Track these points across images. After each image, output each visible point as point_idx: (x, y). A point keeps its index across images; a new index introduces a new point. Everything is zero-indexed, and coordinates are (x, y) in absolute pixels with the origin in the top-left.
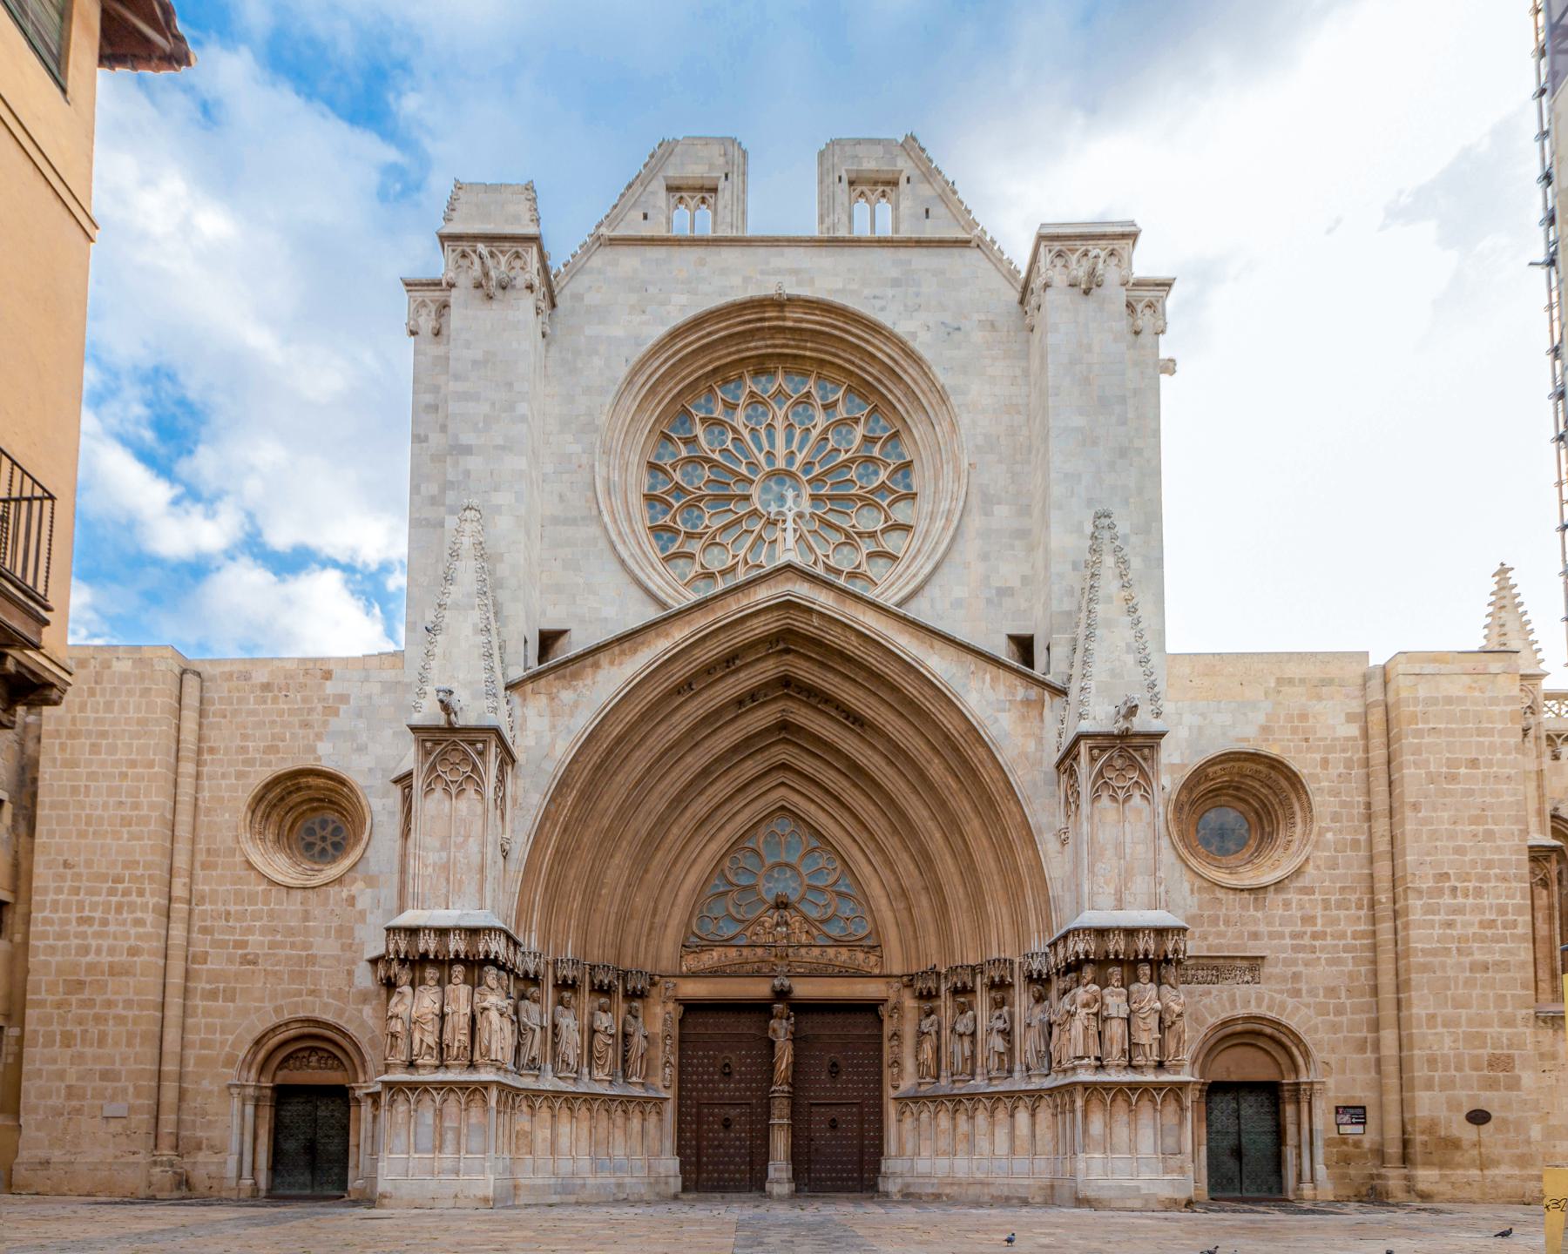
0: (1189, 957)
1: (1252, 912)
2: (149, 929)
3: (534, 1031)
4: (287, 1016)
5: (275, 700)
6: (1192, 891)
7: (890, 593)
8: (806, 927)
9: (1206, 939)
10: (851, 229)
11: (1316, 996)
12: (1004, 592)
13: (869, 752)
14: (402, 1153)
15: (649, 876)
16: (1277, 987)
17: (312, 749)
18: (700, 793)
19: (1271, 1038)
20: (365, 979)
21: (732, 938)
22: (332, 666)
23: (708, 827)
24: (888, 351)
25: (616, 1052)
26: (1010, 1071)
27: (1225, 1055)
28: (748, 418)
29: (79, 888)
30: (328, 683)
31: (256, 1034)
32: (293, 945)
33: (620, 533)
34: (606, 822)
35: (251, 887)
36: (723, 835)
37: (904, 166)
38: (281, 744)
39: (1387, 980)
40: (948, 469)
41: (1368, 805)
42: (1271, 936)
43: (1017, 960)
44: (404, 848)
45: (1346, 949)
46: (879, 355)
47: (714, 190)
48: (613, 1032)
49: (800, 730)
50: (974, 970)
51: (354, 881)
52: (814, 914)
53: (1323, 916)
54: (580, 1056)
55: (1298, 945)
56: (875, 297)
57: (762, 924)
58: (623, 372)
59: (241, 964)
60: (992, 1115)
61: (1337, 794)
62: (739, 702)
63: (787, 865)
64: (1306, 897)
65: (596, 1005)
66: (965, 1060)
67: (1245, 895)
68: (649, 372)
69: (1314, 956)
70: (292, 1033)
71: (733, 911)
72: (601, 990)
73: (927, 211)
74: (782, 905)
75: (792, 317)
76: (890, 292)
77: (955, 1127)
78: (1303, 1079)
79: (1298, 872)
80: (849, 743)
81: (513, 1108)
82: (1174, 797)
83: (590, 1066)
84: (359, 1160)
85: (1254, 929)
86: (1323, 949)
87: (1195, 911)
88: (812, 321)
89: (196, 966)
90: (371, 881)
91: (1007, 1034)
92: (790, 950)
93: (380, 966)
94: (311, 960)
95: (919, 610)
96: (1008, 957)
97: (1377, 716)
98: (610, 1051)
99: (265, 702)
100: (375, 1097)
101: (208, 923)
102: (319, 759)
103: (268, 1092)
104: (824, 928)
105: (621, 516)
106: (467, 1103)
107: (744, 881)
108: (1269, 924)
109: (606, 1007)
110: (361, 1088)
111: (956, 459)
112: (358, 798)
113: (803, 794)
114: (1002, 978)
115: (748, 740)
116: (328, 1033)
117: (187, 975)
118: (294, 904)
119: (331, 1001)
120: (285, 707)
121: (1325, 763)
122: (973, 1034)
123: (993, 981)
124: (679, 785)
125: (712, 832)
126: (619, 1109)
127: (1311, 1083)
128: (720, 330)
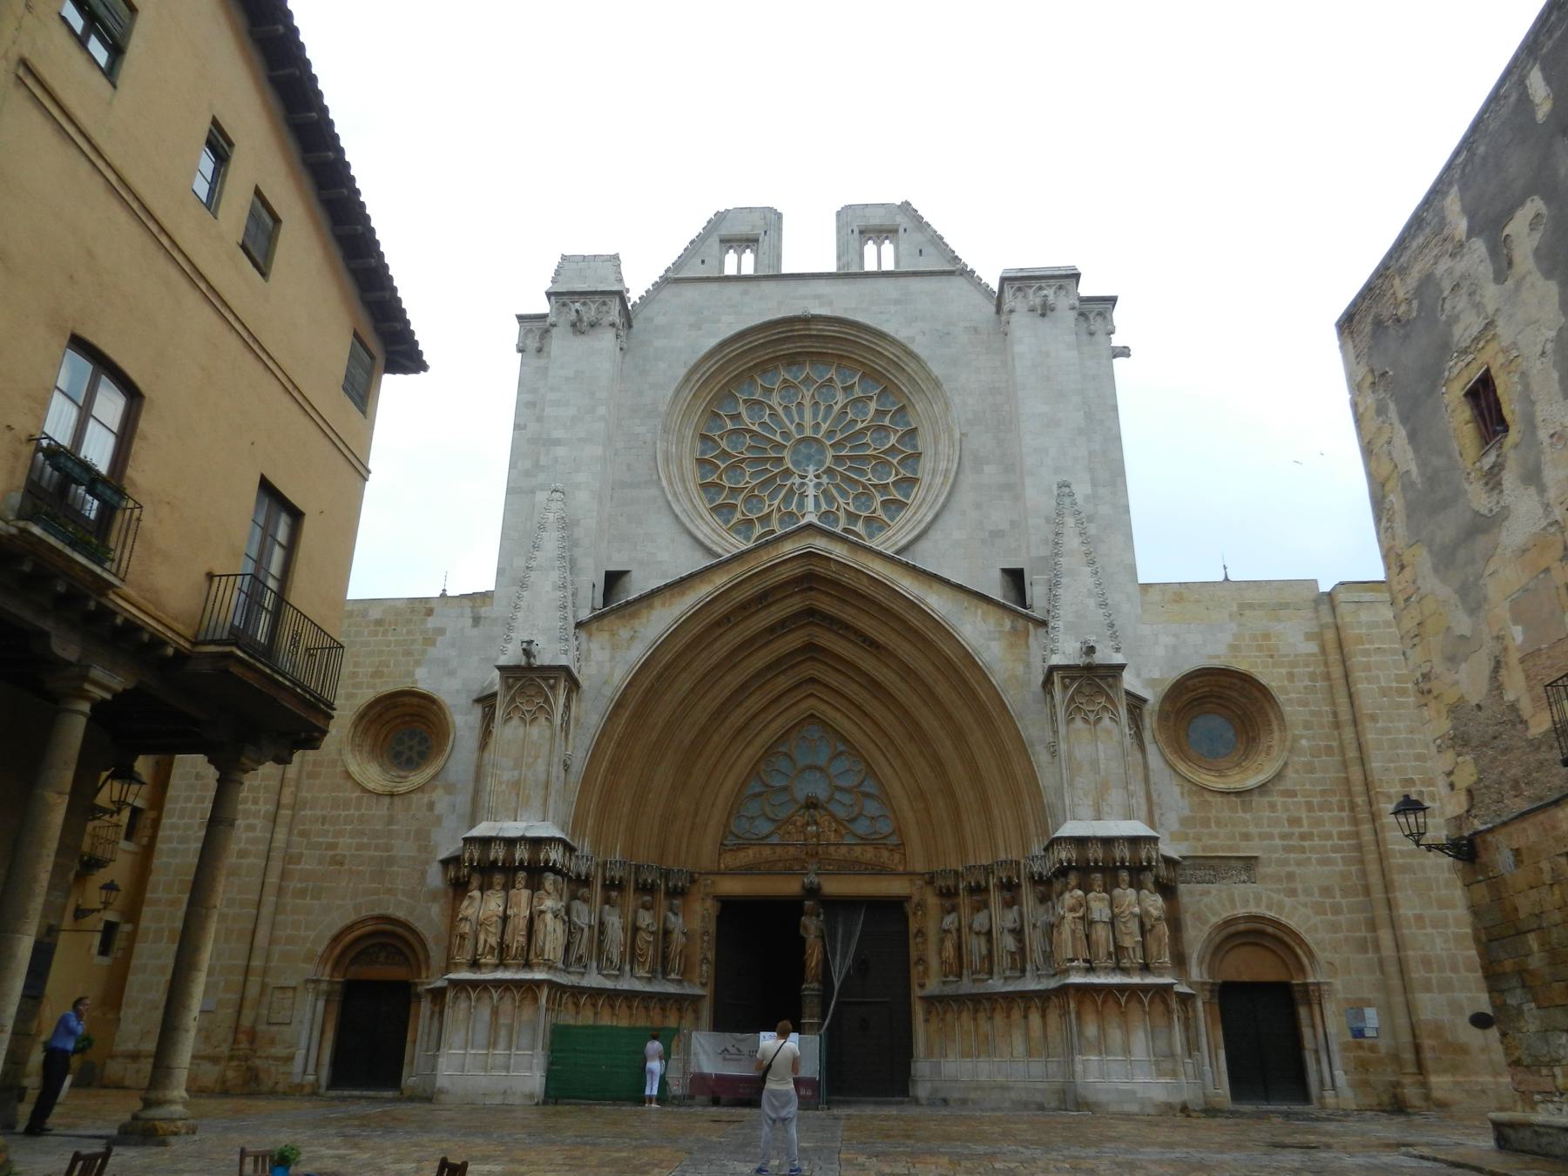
0: (1184, 858)
1: (1241, 814)
2: (258, 834)
3: (583, 930)
4: (364, 913)
5: (385, 633)
6: (1182, 794)
7: (900, 535)
10: (862, 266)
11: (1311, 895)
12: (997, 534)
13: (885, 670)
14: (460, 1049)
17: (410, 674)
19: (1274, 937)
20: (435, 878)
21: (767, 837)
22: (433, 605)
24: (892, 350)
25: (656, 950)
26: (1023, 971)
28: (782, 398)
29: (205, 797)
30: (430, 619)
31: (335, 931)
32: (377, 848)
33: (675, 494)
35: (347, 794)
37: (902, 221)
38: (385, 670)
39: (1375, 879)
40: (944, 438)
41: (1335, 714)
42: (1262, 836)
43: (1022, 862)
44: (480, 758)
45: (1335, 849)
46: (886, 353)
47: (756, 241)
48: (654, 929)
49: (824, 650)
50: (988, 870)
51: (434, 789)
52: (841, 813)
53: (1307, 817)
54: (623, 954)
56: (881, 313)
58: (682, 372)
59: (330, 864)
60: (1008, 1017)
61: (1306, 704)
62: (771, 629)
64: (1290, 800)
65: (640, 902)
66: (982, 959)
67: (1233, 798)
68: (702, 372)
69: (1304, 856)
70: (368, 929)
71: (768, 810)
72: (645, 889)
73: (921, 251)
74: (812, 804)
75: (815, 329)
76: (893, 309)
77: (977, 1027)
78: (1311, 980)
79: (1279, 776)
80: (868, 663)
81: (560, 1005)
82: (1157, 708)
83: (632, 963)
84: (416, 1053)
85: (1244, 830)
86: (1313, 849)
87: (1187, 813)
88: (830, 330)
89: (291, 866)
90: (450, 789)
91: (1018, 933)
93: (451, 867)
94: (391, 861)
95: (925, 558)
96: (1014, 858)
97: (1330, 635)
98: (651, 948)
99: (376, 635)
100: (438, 995)
101: (307, 827)
102: (416, 682)
103: (338, 987)
104: (850, 826)
105: (676, 481)
106: (521, 1001)
109: (648, 905)
110: (422, 984)
111: (950, 431)
112: (444, 714)
114: (1010, 879)
115: (779, 661)
116: (400, 930)
117: (284, 875)
118: (381, 810)
119: (404, 899)
120: (392, 638)
121: (1291, 677)
122: (989, 933)
123: (1001, 881)
125: (749, 739)
127: (1318, 984)
128: (760, 339)
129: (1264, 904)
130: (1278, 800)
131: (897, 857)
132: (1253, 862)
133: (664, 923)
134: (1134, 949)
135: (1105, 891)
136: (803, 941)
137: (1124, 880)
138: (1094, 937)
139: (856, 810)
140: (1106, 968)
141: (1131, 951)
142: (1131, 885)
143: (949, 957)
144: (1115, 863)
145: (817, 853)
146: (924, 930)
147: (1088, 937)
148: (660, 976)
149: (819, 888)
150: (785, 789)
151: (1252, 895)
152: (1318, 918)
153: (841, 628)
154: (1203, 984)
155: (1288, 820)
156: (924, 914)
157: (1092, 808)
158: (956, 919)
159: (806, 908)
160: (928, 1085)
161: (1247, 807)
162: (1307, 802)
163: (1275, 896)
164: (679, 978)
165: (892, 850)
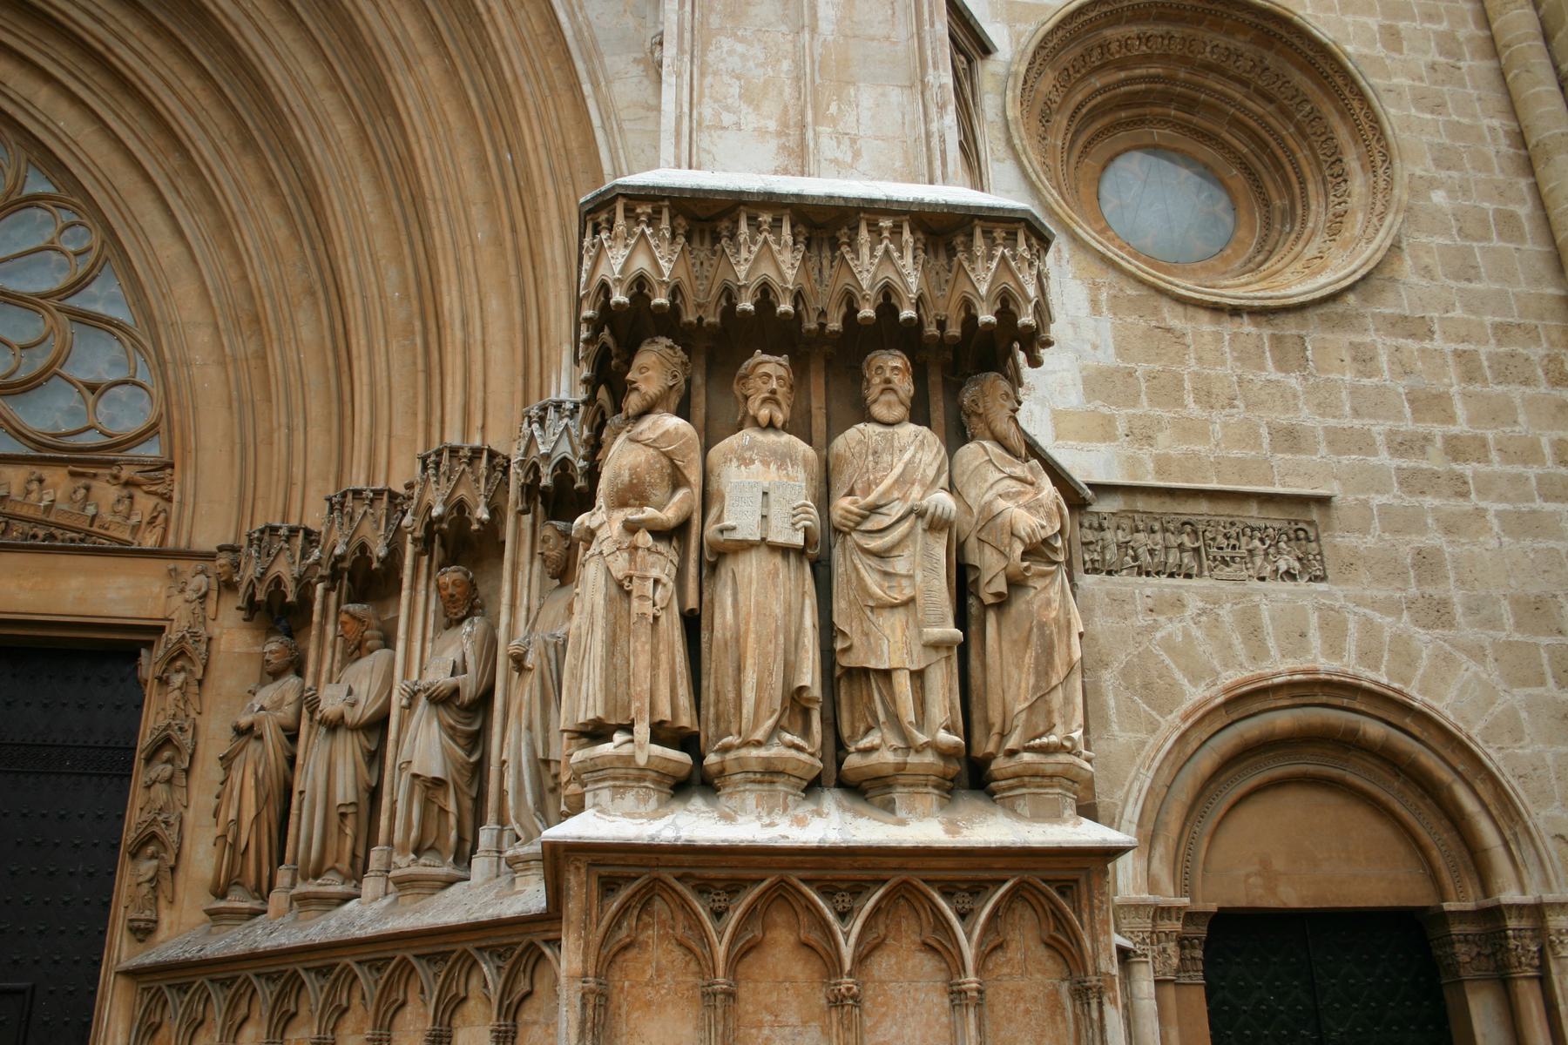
6: (1094, 303)
9: (1149, 439)
11: (1493, 623)
16: (1380, 593)
19: (1387, 758)
27: (1253, 817)
42: (1338, 440)
55: (1415, 472)
61: (1438, 107)
64: (1412, 345)
67: (1247, 326)
69: (1467, 505)
78: (1510, 895)
85: (1283, 419)
87: (1107, 357)
108: (1323, 408)
129: (1351, 645)
130: (1382, 344)
132: (1315, 514)
134: (918, 676)
135: (799, 426)
137: (888, 386)
138: (723, 618)
140: (770, 773)
141: (903, 684)
142: (919, 413)
144: (852, 311)
147: (692, 624)
151: (1314, 619)
152: (1520, 693)
154: (1162, 912)
155: (1411, 402)
157: (773, 144)
161: (1290, 355)
162: (1458, 354)
163: (1385, 621)
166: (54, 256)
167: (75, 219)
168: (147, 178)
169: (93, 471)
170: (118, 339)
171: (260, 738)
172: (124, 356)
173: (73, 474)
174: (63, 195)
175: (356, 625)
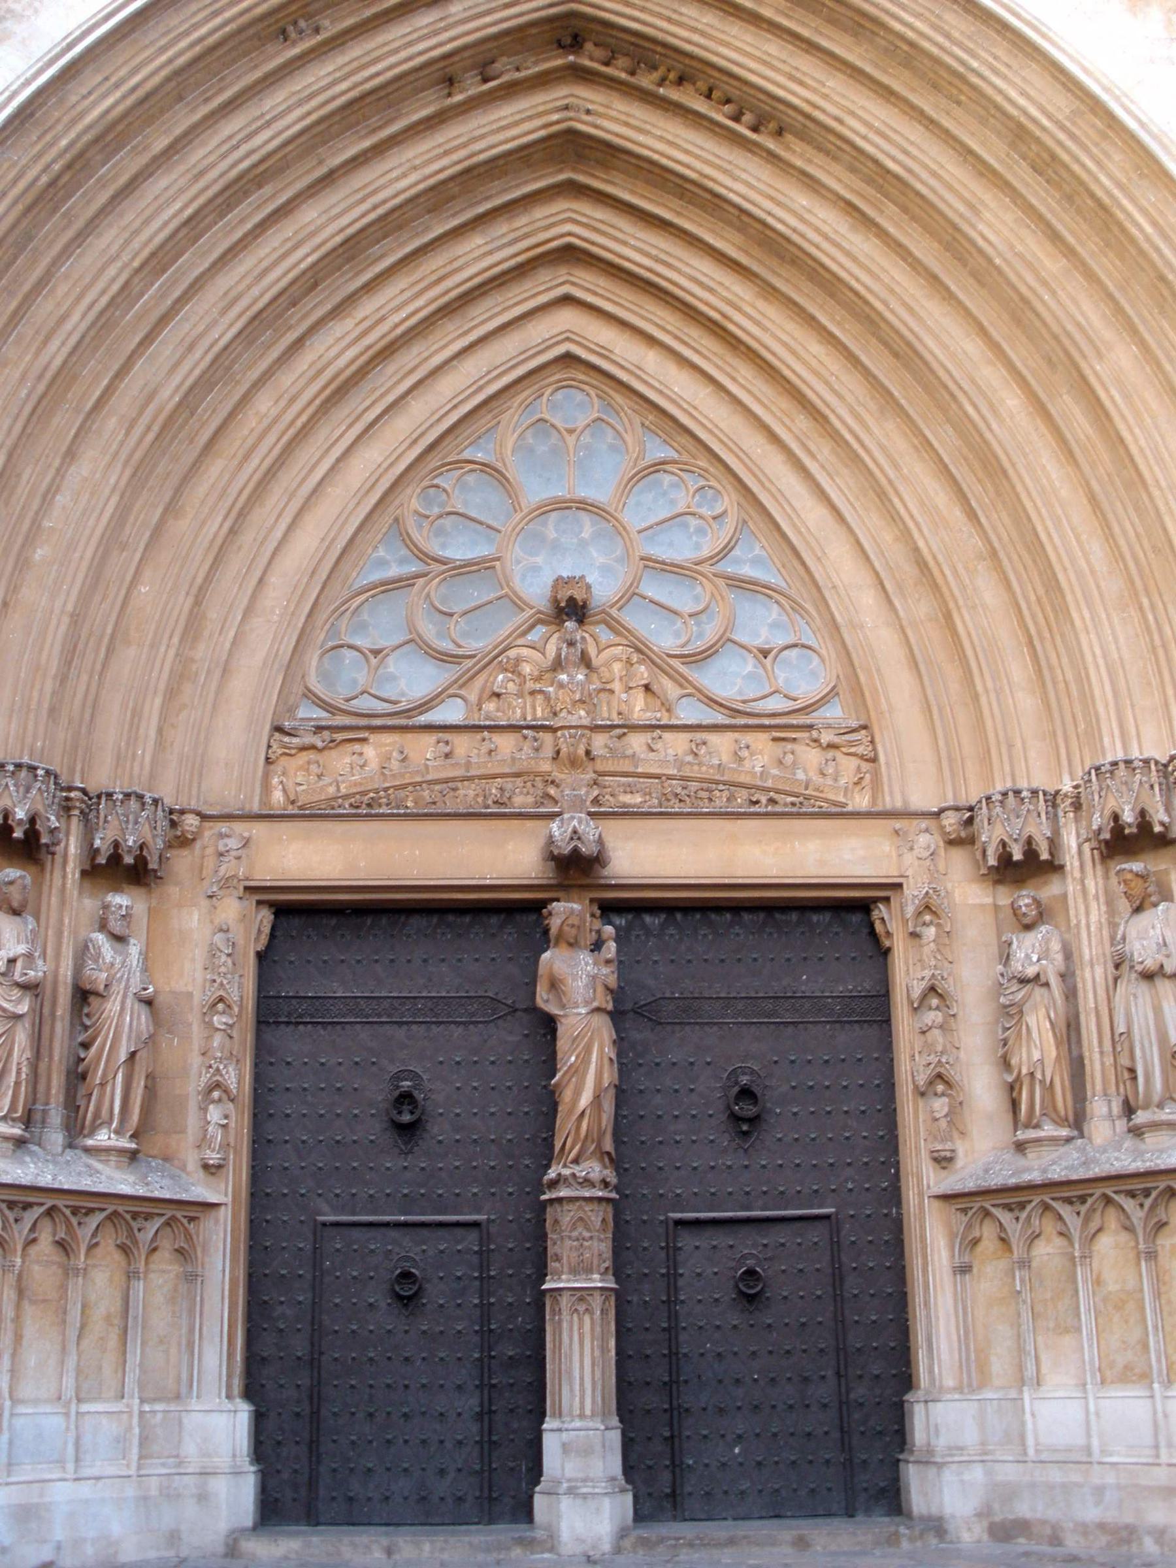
8: (643, 672)
15: (181, 526)
18: (337, 312)
21: (426, 705)
23: (355, 402)
34: (56, 351)
36: (403, 425)
57: (514, 668)
63: (584, 505)
71: (428, 629)
92: (599, 742)
98: (22, 1037)
107: (460, 549)
113: (623, 324)
124: (279, 277)
126: (45, 1238)
131: (849, 766)
133: (78, 969)
136: (549, 1024)
139: (710, 631)
143: (1041, 1061)
145: (588, 753)
146: (948, 986)
148: (56, 1138)
149: (598, 860)
150: (483, 567)
153: (661, 82)
156: (946, 936)
158: (1055, 946)
159: (555, 923)
160: (977, 1474)
164: (126, 1143)
165: (832, 746)
166: (693, 522)
167: (702, 483)
168: (774, 438)
169: (794, 735)
170: (777, 602)
171: (1047, 985)
172: (785, 618)
173: (775, 739)
174: (685, 457)
175: (1140, 881)
